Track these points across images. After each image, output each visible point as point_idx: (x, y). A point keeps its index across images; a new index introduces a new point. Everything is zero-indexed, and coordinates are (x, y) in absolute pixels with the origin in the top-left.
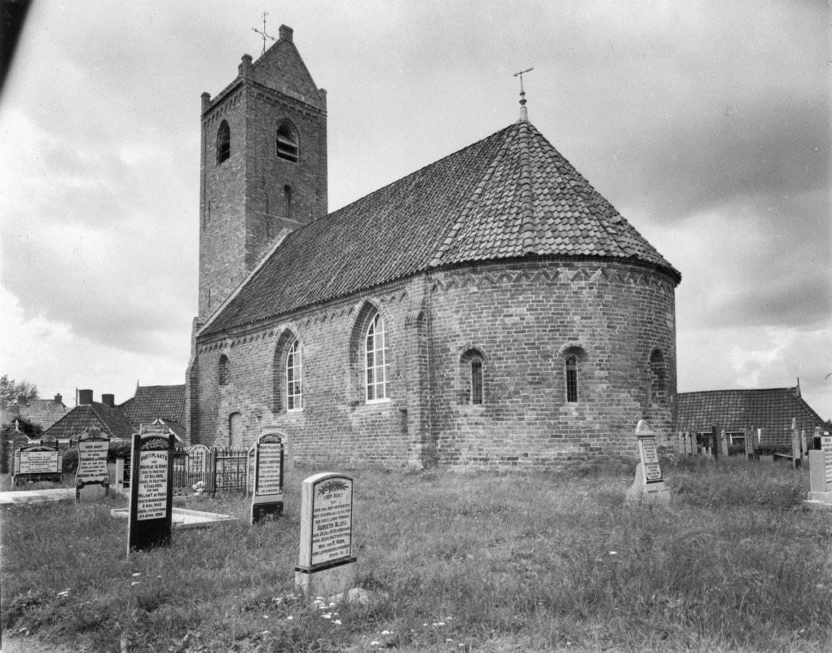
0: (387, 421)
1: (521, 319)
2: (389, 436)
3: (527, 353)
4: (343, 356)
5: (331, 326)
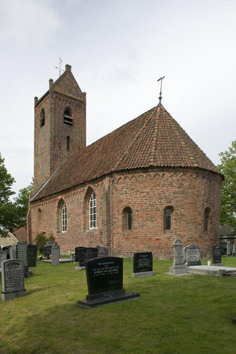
3: (149, 208)
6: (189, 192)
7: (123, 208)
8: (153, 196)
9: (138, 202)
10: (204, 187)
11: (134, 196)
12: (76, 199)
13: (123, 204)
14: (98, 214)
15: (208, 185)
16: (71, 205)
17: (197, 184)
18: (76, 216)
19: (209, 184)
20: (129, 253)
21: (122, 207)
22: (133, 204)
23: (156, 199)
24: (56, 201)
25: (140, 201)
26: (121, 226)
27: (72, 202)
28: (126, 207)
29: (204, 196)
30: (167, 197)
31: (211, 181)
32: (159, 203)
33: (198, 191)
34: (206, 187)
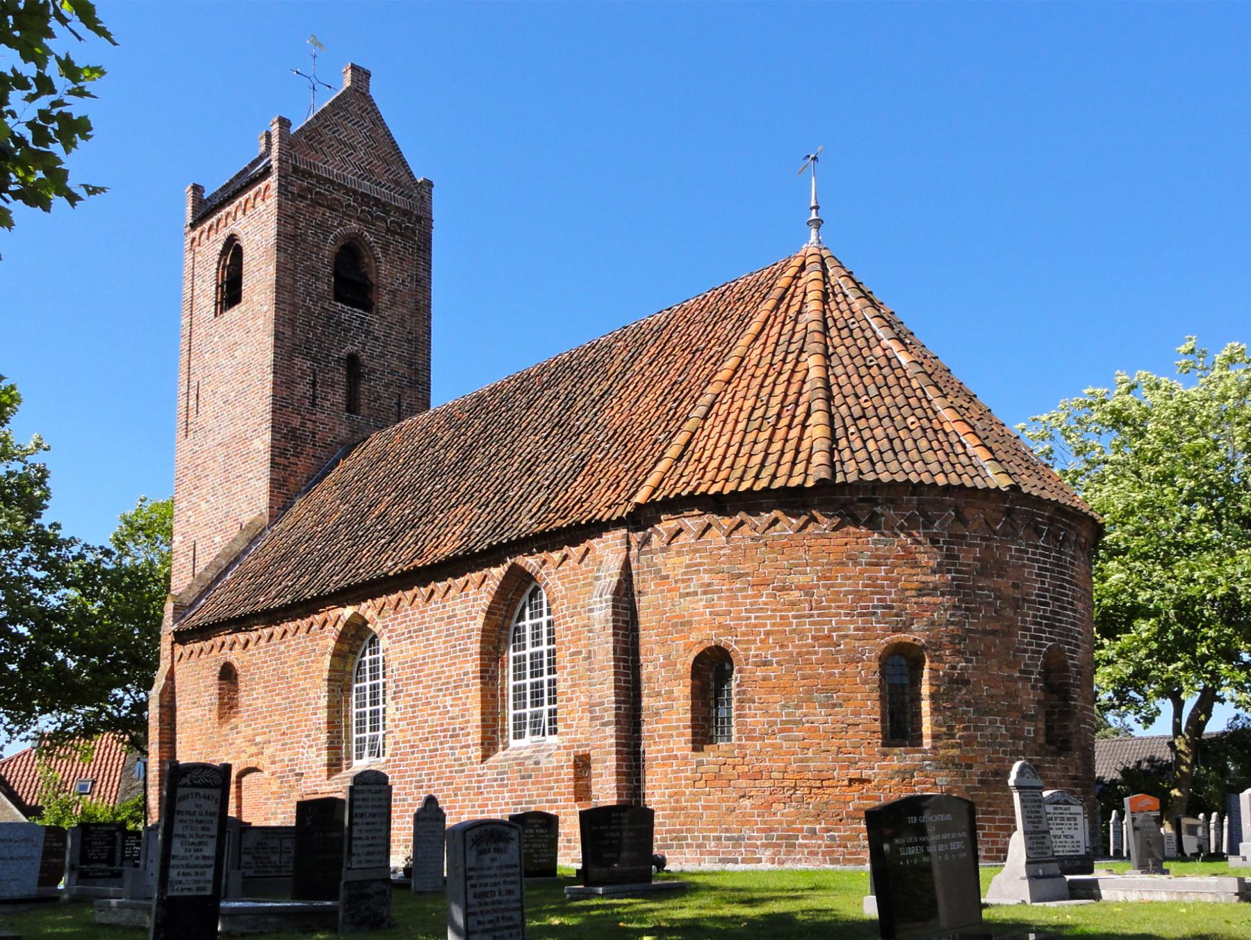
0: (552, 775)
1: (806, 594)
2: (556, 801)
3: (816, 653)
4: (467, 662)
5: (444, 607)
6: (982, 588)
7: (695, 653)
8: (832, 601)
9: (765, 625)
10: (1040, 568)
11: (744, 604)
12: (442, 619)
13: (694, 637)
14: (565, 680)
15: (1051, 564)
16: (412, 643)
17: (1011, 557)
18: (440, 690)
19: (1055, 558)
20: (728, 839)
21: (688, 648)
22: (743, 634)
23: (847, 615)
24: (329, 627)
25: (773, 625)
26: (685, 727)
27: (421, 630)
28: (709, 649)
29: (1041, 603)
30: (891, 607)
31: (1062, 543)
32: (857, 629)
33: (1015, 586)
34: (1047, 570)
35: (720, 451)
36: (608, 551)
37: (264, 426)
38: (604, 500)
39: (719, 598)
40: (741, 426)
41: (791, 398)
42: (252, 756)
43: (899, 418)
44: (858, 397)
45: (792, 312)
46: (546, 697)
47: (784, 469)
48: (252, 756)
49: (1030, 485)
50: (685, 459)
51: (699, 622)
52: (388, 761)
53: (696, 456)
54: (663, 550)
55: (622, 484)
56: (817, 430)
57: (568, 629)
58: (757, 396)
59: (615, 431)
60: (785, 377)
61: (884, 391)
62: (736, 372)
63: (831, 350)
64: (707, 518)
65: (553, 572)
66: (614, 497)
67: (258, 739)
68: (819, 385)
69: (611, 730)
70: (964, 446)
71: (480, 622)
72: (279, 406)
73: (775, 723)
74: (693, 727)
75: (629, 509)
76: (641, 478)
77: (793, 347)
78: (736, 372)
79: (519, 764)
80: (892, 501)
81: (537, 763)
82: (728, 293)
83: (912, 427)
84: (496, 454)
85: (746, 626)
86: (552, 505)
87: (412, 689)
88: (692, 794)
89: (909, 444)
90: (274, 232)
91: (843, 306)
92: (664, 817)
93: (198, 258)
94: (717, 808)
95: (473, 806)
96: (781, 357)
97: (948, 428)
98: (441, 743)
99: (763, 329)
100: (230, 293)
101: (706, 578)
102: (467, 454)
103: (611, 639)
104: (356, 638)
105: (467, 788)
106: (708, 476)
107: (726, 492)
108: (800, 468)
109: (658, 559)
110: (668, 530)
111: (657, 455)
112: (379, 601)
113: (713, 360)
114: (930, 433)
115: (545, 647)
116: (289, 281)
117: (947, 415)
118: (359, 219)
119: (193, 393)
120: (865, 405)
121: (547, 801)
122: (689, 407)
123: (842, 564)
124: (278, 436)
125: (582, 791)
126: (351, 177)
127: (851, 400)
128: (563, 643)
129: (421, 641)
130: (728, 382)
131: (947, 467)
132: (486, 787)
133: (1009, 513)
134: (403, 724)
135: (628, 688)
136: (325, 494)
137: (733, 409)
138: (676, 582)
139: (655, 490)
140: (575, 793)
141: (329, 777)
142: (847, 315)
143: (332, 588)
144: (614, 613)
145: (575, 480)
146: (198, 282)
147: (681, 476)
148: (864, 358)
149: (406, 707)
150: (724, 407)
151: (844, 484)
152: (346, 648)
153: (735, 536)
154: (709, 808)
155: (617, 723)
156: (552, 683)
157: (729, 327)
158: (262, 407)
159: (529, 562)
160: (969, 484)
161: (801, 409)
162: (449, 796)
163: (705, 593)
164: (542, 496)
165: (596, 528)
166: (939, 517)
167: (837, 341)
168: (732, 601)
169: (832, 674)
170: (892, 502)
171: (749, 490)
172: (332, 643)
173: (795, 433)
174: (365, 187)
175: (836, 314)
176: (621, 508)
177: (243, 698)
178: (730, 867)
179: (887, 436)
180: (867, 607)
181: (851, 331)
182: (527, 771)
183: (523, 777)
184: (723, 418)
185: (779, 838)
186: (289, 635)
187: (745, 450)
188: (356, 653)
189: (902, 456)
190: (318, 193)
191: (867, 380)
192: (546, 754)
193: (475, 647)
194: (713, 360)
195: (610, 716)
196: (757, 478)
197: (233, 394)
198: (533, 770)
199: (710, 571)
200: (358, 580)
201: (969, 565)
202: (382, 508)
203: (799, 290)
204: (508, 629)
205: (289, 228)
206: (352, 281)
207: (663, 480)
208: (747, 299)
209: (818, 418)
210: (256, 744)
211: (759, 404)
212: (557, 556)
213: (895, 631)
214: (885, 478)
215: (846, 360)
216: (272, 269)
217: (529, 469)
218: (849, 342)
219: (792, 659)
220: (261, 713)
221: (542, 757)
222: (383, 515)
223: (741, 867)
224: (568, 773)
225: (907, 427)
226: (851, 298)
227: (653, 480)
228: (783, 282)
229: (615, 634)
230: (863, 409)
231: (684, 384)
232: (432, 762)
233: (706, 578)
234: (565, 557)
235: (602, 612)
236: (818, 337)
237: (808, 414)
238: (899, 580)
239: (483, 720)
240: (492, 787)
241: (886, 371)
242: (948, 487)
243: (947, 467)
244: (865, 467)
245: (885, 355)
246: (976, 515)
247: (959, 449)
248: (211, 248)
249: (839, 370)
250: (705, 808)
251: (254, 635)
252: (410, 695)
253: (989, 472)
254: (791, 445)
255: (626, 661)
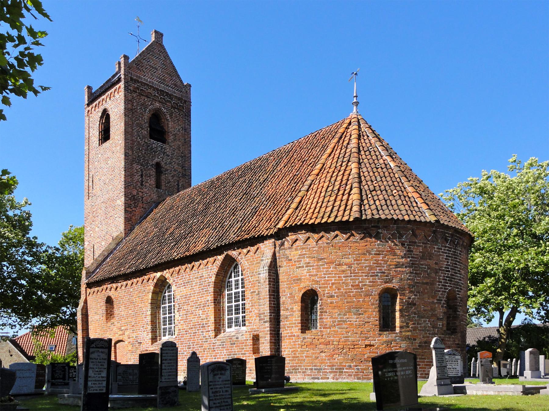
0: (243, 343)
1: (349, 267)
2: (245, 354)
3: (352, 292)
4: (208, 296)
5: (198, 272)
7: (302, 292)
9: (332, 280)
11: (323, 271)
12: (198, 278)
13: (302, 285)
14: (249, 304)
16: (185, 288)
18: (197, 308)
20: (315, 369)
21: (300, 290)
22: (323, 284)
23: (366, 276)
24: (151, 281)
25: (335, 280)
26: (298, 323)
27: (189, 282)
28: (308, 290)
30: (384, 273)
32: (370, 282)
35: (314, 205)
36: (266, 248)
37: (121, 194)
38: (265, 226)
39: (313, 269)
40: (323, 194)
41: (344, 182)
42: (120, 335)
43: (389, 191)
44: (372, 182)
45: (345, 144)
46: (241, 311)
47: (341, 213)
48: (120, 335)
49: (444, 220)
50: (299, 208)
51: (304, 279)
52: (176, 337)
53: (304, 208)
54: (289, 248)
55: (272, 220)
56: (355, 196)
57: (250, 282)
58: (330, 181)
59: (270, 197)
60: (341, 173)
61: (384, 179)
62: (321, 170)
63: (361, 161)
64: (308, 235)
65: (243, 257)
66: (269, 225)
67: (123, 328)
68: (356, 176)
69: (268, 324)
70: (417, 203)
71: (213, 279)
72: (127, 186)
73: (335, 321)
74: (301, 323)
75: (275, 230)
76: (280, 217)
77: (345, 159)
78: (321, 170)
79: (230, 339)
80: (386, 227)
81: (237, 338)
82: (318, 135)
83: (395, 195)
84: (220, 206)
85: (324, 280)
86: (243, 229)
87: (185, 307)
88: (301, 351)
89: (393, 202)
90: (123, 108)
91: (367, 141)
92: (289, 360)
93: (91, 120)
94: (311, 357)
95: (211, 356)
96: (340, 164)
97: (410, 195)
98: (198, 330)
99: (332, 151)
100: (105, 135)
101: (307, 260)
102: (207, 207)
103: (268, 286)
104: (162, 286)
105: (209, 349)
106: (309, 216)
107: (316, 223)
108: (347, 213)
109: (287, 252)
110: (291, 240)
111: (287, 207)
112: (171, 270)
113: (311, 165)
114: (402, 197)
115: (240, 290)
116: (130, 130)
117: (410, 189)
118: (159, 102)
119: (91, 180)
120: (375, 185)
121: (242, 354)
122: (301, 186)
123: (364, 254)
124: (127, 199)
125: (256, 350)
126: (156, 83)
127: (369, 183)
128: (248, 288)
129: (189, 287)
130: (318, 175)
131: (409, 212)
132: (216, 348)
133: (434, 232)
134: (182, 322)
135: (274, 307)
136: (148, 224)
137: (319, 187)
138: (295, 262)
139: (286, 222)
140: (253, 351)
141: (152, 344)
142: (368, 145)
143: (151, 264)
144: (269, 275)
145: (253, 218)
146: (91, 130)
147: (297, 216)
148: (375, 164)
149: (183, 315)
150: (316, 186)
151: (366, 219)
152: (158, 290)
153: (320, 242)
154: (308, 357)
155: (270, 321)
156: (244, 305)
157: (318, 150)
158: (120, 186)
159: (234, 253)
160: (418, 219)
161: (348, 187)
162: (201, 352)
163: (307, 267)
164: (239, 225)
165: (261, 239)
166: (405, 234)
167: (364, 157)
168: (318, 270)
169: (359, 301)
170: (386, 228)
171: (326, 222)
172: (152, 288)
173: (345, 197)
174: (162, 87)
175: (364, 145)
176: (272, 230)
177: (116, 311)
178: (316, 381)
179: (384, 199)
180: (374, 273)
181: (370, 152)
182: (233, 341)
183: (232, 344)
184: (315, 191)
185: (336, 369)
186: (134, 285)
187: (324, 205)
188: (162, 292)
189: (390, 207)
190: (141, 90)
191: (376, 174)
192: (241, 334)
193: (211, 290)
194: (311, 165)
195: (267, 318)
196: (329, 217)
197: (108, 180)
198: (236, 341)
199: (309, 257)
200: (163, 261)
201: (417, 255)
202: (172, 230)
203: (348, 134)
204: (225, 282)
205: (130, 106)
206: (157, 130)
207: (290, 218)
208: (326, 138)
209: (355, 190)
210: (122, 330)
211: (330, 185)
212: (245, 251)
213: (386, 283)
214: (383, 217)
215: (368, 165)
216: (123, 124)
217: (233, 213)
218: (369, 157)
219: (342, 295)
220: (123, 317)
221: (239, 336)
222: (172, 233)
223: (321, 381)
224: (250, 342)
225: (393, 195)
226: (370, 138)
227: (285, 218)
228: (341, 130)
229: (269, 284)
230: (375, 187)
231: (299, 176)
232: (194, 338)
233: (307, 260)
234: (249, 251)
235: (264, 275)
236: (356, 155)
237: (351, 189)
238: (388, 261)
239: (215, 320)
240: (219, 348)
241: (385, 170)
242: (409, 221)
243: (409, 212)
244: (375, 212)
245: (384, 163)
246: (421, 233)
247: (415, 205)
248: (97, 115)
249: (365, 170)
250: (306, 357)
251: (119, 284)
252: (185, 310)
253: (427, 214)
254: (344, 202)
255: (274, 295)
